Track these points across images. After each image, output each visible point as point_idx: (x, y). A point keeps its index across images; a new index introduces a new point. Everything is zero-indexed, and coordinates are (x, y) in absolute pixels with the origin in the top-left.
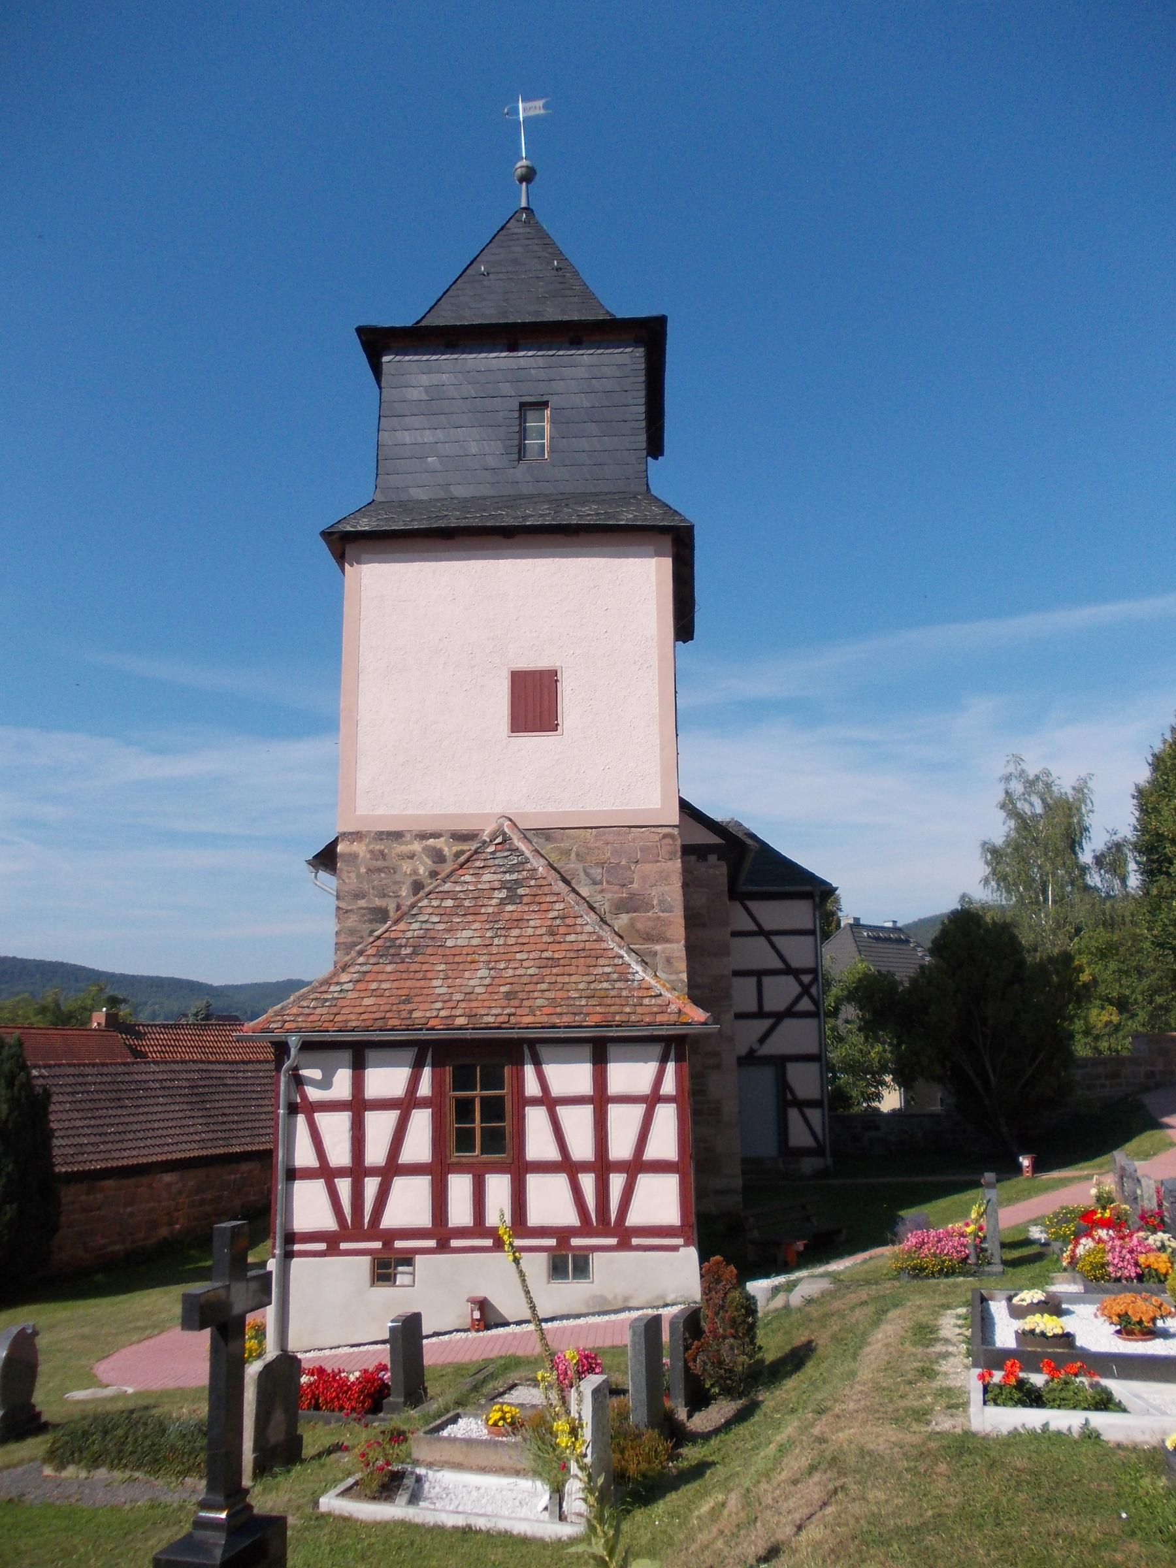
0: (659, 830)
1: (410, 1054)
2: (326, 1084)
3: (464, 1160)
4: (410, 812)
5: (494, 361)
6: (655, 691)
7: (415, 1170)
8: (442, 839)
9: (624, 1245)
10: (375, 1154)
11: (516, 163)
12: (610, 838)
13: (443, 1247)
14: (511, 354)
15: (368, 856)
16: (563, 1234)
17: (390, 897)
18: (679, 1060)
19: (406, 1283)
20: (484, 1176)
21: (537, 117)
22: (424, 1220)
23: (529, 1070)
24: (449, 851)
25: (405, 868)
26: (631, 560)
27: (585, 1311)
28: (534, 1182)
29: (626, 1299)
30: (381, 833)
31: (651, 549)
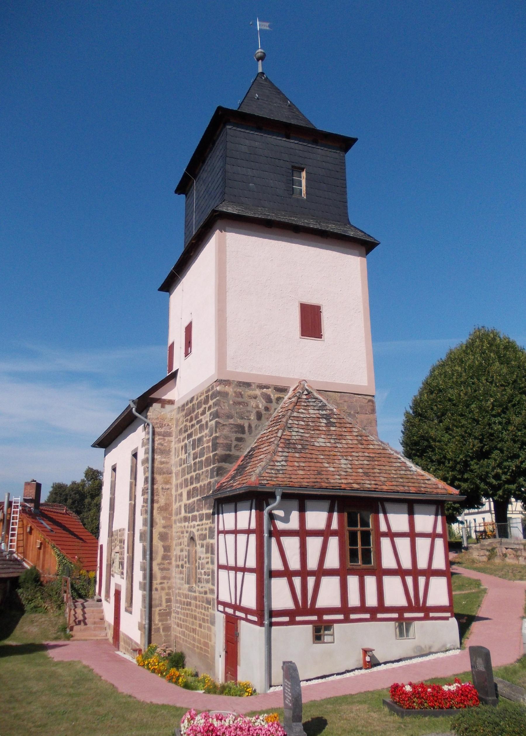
0: (366, 397)
1: (326, 504)
2: (286, 519)
3: (354, 567)
4: (254, 372)
5: (279, 142)
6: (362, 325)
7: (331, 573)
8: (270, 389)
9: (426, 618)
10: (312, 564)
11: (256, 51)
12: (346, 399)
13: (347, 620)
14: (287, 140)
15: (234, 395)
16: (400, 610)
17: (245, 419)
18: (443, 515)
19: (329, 641)
20: (364, 576)
21: (266, 30)
22: (337, 603)
23: (381, 516)
24: (274, 397)
25: (252, 403)
26: (349, 256)
27: (413, 655)
28: (387, 580)
29: (430, 648)
30: (240, 382)
31: (357, 252)
